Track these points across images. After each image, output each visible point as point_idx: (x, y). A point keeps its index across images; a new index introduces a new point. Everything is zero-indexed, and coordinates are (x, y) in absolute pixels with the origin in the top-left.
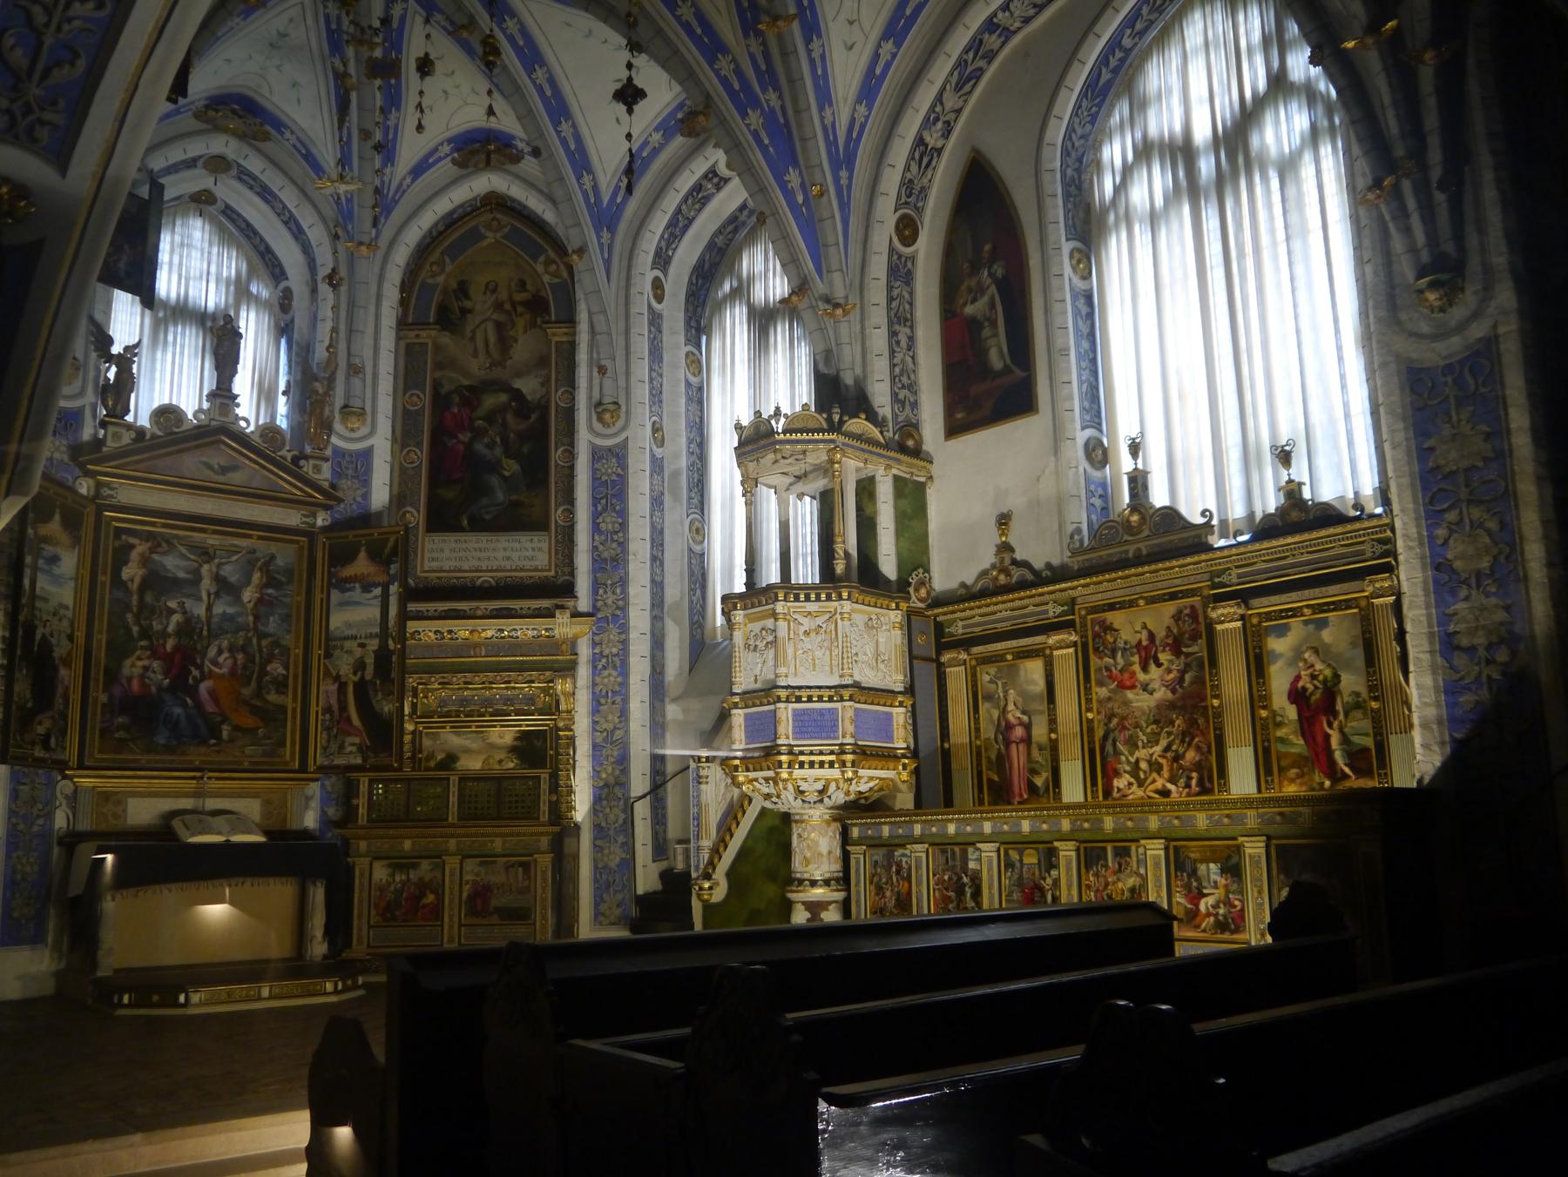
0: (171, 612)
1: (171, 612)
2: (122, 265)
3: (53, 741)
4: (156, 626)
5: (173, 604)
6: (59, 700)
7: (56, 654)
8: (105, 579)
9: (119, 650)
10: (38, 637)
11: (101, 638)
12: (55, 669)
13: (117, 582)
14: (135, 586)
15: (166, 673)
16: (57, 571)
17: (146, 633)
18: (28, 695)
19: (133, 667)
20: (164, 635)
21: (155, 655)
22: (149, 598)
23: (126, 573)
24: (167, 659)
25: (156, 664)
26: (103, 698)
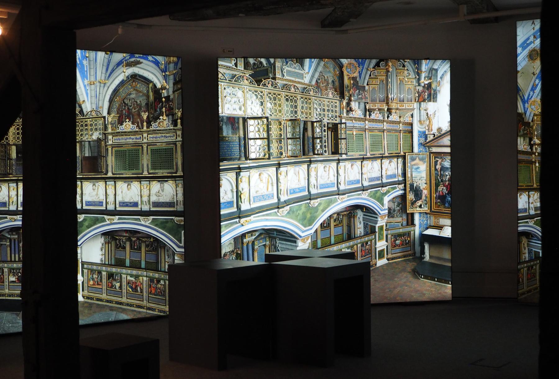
0: (447, 175)
1: (447, 175)
2: (426, 97)
3: (423, 206)
4: (444, 179)
5: (447, 174)
6: (424, 197)
7: (421, 188)
8: (433, 168)
9: (437, 185)
10: (415, 185)
11: (433, 182)
12: (422, 191)
13: (436, 170)
14: (439, 170)
15: (447, 190)
16: (418, 170)
17: (442, 181)
18: (413, 198)
19: (440, 188)
20: (446, 181)
21: (444, 186)
22: (442, 172)
23: (437, 167)
24: (447, 187)
25: (445, 188)
26: (435, 196)
